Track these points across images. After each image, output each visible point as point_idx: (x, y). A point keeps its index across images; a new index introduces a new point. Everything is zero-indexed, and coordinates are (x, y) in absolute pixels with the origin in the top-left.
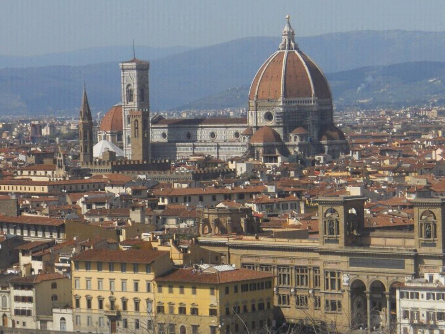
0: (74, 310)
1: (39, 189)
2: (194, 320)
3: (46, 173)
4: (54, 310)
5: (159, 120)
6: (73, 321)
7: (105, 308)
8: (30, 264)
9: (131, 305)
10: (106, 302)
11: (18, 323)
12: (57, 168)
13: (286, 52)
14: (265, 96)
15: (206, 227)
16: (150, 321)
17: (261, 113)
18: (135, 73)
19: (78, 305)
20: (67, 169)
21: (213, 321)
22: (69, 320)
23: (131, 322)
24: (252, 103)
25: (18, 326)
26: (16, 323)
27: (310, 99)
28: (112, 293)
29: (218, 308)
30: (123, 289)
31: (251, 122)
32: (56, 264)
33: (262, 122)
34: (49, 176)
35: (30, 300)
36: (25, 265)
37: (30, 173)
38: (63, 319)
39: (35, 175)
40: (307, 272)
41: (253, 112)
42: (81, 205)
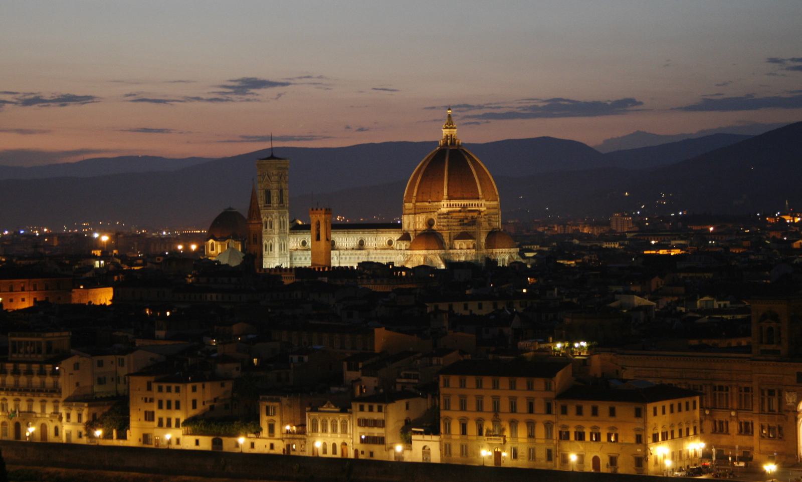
0: (442, 436)
4: (414, 437)
6: (440, 450)
8: (359, 380)
14: (425, 198)
17: (421, 217)
19: (448, 431)
21: (639, 450)
23: (523, 450)
25: (361, 457)
26: (360, 452)
30: (513, 409)
32: (398, 380)
40: (727, 390)
41: (411, 216)
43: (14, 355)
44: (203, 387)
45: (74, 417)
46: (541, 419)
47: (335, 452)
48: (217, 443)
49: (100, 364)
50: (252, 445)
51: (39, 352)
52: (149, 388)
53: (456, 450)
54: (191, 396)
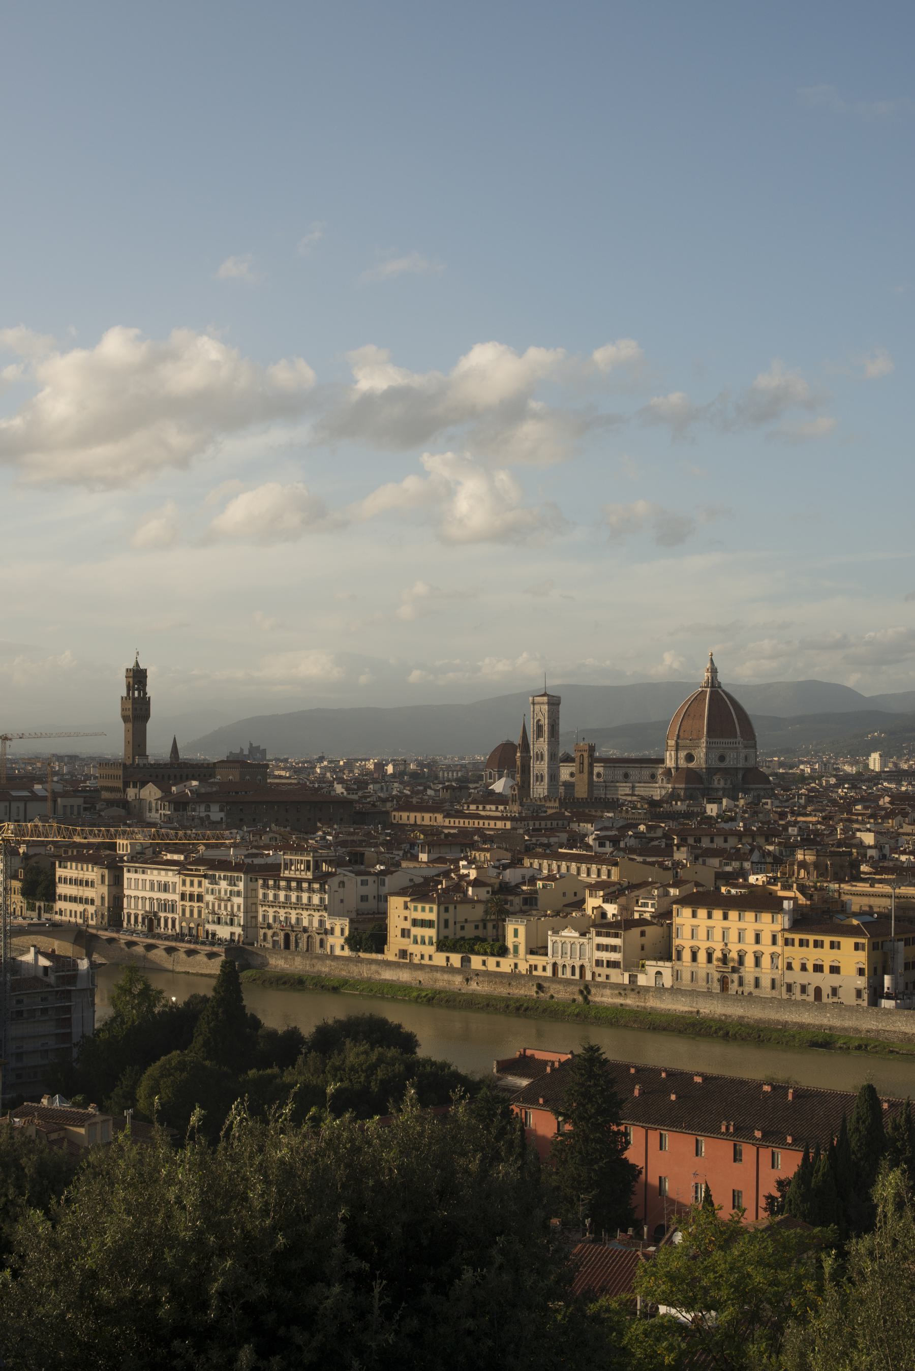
1: (500, 824)
2: (835, 980)
3: (497, 808)
5: (568, 759)
7: (715, 962)
8: (600, 907)
9: (749, 960)
10: (718, 954)
11: (599, 975)
12: (510, 802)
13: (708, 690)
15: (802, 871)
16: (773, 981)
18: (546, 707)
19: (679, 958)
20: (521, 805)
22: (667, 974)
24: (672, 743)
25: (598, 979)
27: (734, 740)
28: (726, 944)
29: (866, 967)
31: (670, 763)
32: (636, 909)
33: (682, 763)
34: (502, 812)
35: (614, 949)
36: (593, 908)
37: (478, 807)
38: (659, 973)
39: (484, 809)
42: (591, 842)
43: (286, 872)
44: (455, 908)
45: (337, 931)
46: (766, 948)
47: (573, 974)
48: (466, 961)
49: (364, 883)
50: (498, 964)
51: (308, 869)
52: (406, 908)
53: (686, 976)
54: (445, 916)
